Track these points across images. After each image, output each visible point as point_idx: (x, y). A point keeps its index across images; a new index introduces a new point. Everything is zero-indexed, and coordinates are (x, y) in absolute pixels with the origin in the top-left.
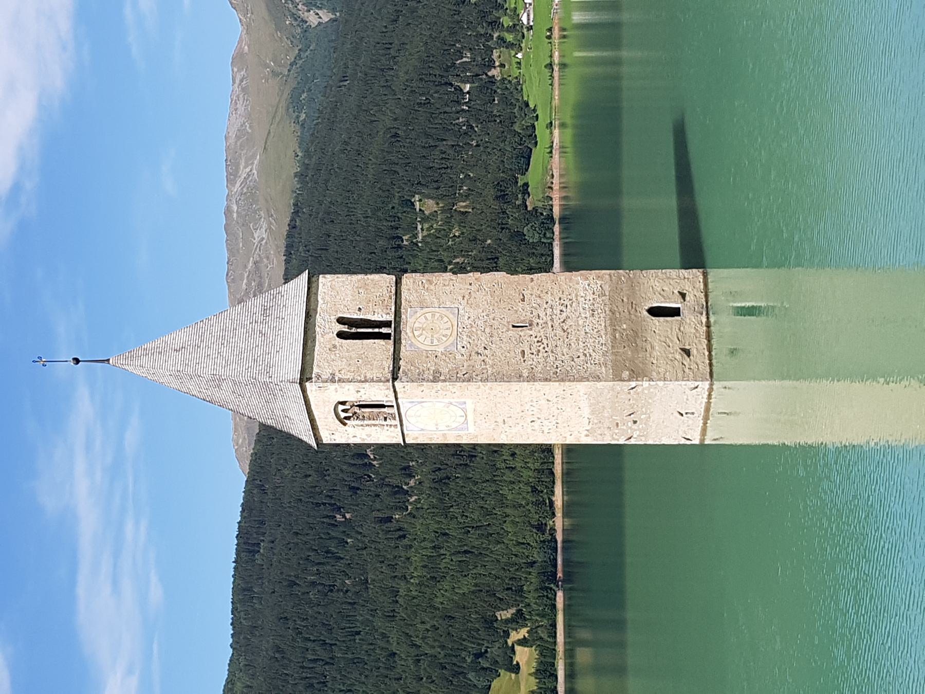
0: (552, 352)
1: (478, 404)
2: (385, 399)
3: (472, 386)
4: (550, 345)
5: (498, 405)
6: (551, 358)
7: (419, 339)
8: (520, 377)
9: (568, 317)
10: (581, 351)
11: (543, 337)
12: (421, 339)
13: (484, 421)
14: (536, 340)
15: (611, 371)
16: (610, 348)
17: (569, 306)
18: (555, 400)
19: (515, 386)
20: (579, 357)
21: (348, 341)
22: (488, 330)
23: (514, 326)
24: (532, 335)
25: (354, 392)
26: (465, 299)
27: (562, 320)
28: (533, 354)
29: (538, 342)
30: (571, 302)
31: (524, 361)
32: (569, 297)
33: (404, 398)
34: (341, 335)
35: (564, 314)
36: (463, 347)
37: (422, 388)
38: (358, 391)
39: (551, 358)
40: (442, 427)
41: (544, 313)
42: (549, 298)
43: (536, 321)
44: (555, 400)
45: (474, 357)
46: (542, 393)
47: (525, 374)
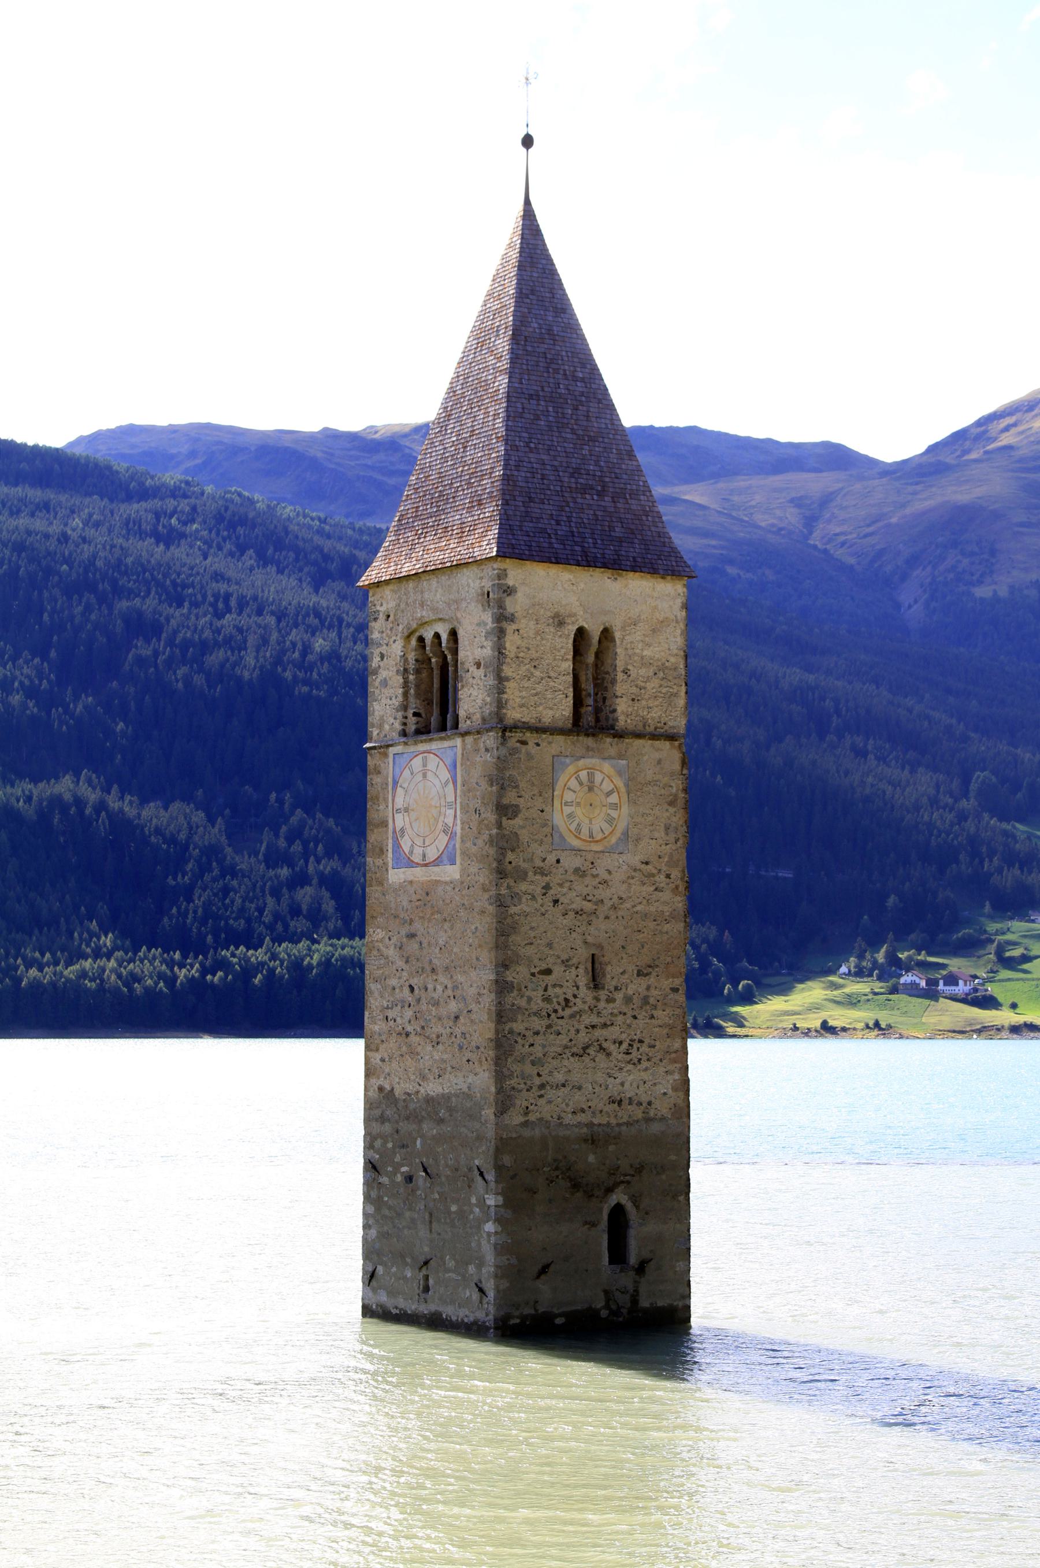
0: (549, 1026)
1: (449, 888)
2: (462, 713)
3: (483, 876)
4: (560, 1021)
5: (447, 925)
6: (538, 1024)
7: (573, 778)
8: (503, 966)
9: (609, 1054)
10: (549, 1079)
11: (575, 1009)
12: (573, 783)
13: (414, 898)
14: (570, 997)
15: (514, 1135)
16: (553, 1134)
17: (628, 1057)
18: (458, 1031)
19: (487, 957)
20: (539, 1075)
21: (570, 646)
22: (588, 906)
23: (593, 955)
24: (578, 988)
26: (643, 866)
27: (605, 1045)
28: (546, 990)
29: (567, 1000)
30: (636, 1061)
31: (533, 975)
32: (644, 1058)
33: (464, 749)
34: (581, 634)
35: (613, 1048)
36: (558, 861)
37: (484, 785)
38: (478, 665)
39: (538, 1024)
40: (400, 821)
41: (615, 1011)
42: (641, 1022)
43: (603, 994)
44: (458, 1031)
45: (542, 880)
46: (473, 1006)
47: (510, 976)
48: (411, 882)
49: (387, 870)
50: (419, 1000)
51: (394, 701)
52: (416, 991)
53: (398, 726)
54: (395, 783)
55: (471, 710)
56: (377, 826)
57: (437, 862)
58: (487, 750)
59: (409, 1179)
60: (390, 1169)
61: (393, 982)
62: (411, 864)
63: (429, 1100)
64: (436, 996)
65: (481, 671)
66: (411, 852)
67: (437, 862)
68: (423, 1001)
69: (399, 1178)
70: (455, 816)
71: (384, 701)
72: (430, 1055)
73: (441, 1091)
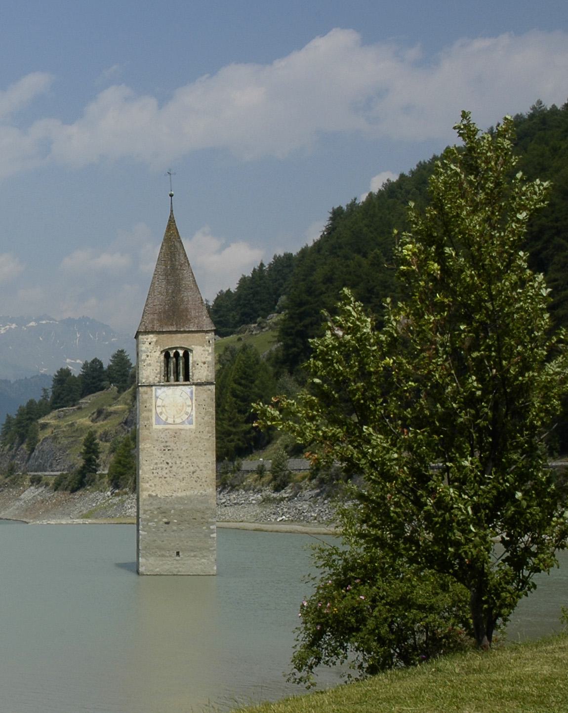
25: (204, 360)
48: (166, 429)
49: (152, 426)
50: (171, 467)
51: (155, 371)
52: (170, 464)
53: (157, 379)
54: (157, 397)
55: (200, 377)
56: (146, 411)
57: (183, 423)
58: (209, 390)
59: (167, 523)
60: (155, 520)
61: (156, 461)
62: (166, 423)
63: (177, 498)
64: (182, 466)
65: (206, 365)
66: (167, 420)
67: (179, 424)
68: (174, 465)
69: (161, 523)
70: (192, 409)
71: (149, 371)
72: (177, 484)
73: (185, 494)
